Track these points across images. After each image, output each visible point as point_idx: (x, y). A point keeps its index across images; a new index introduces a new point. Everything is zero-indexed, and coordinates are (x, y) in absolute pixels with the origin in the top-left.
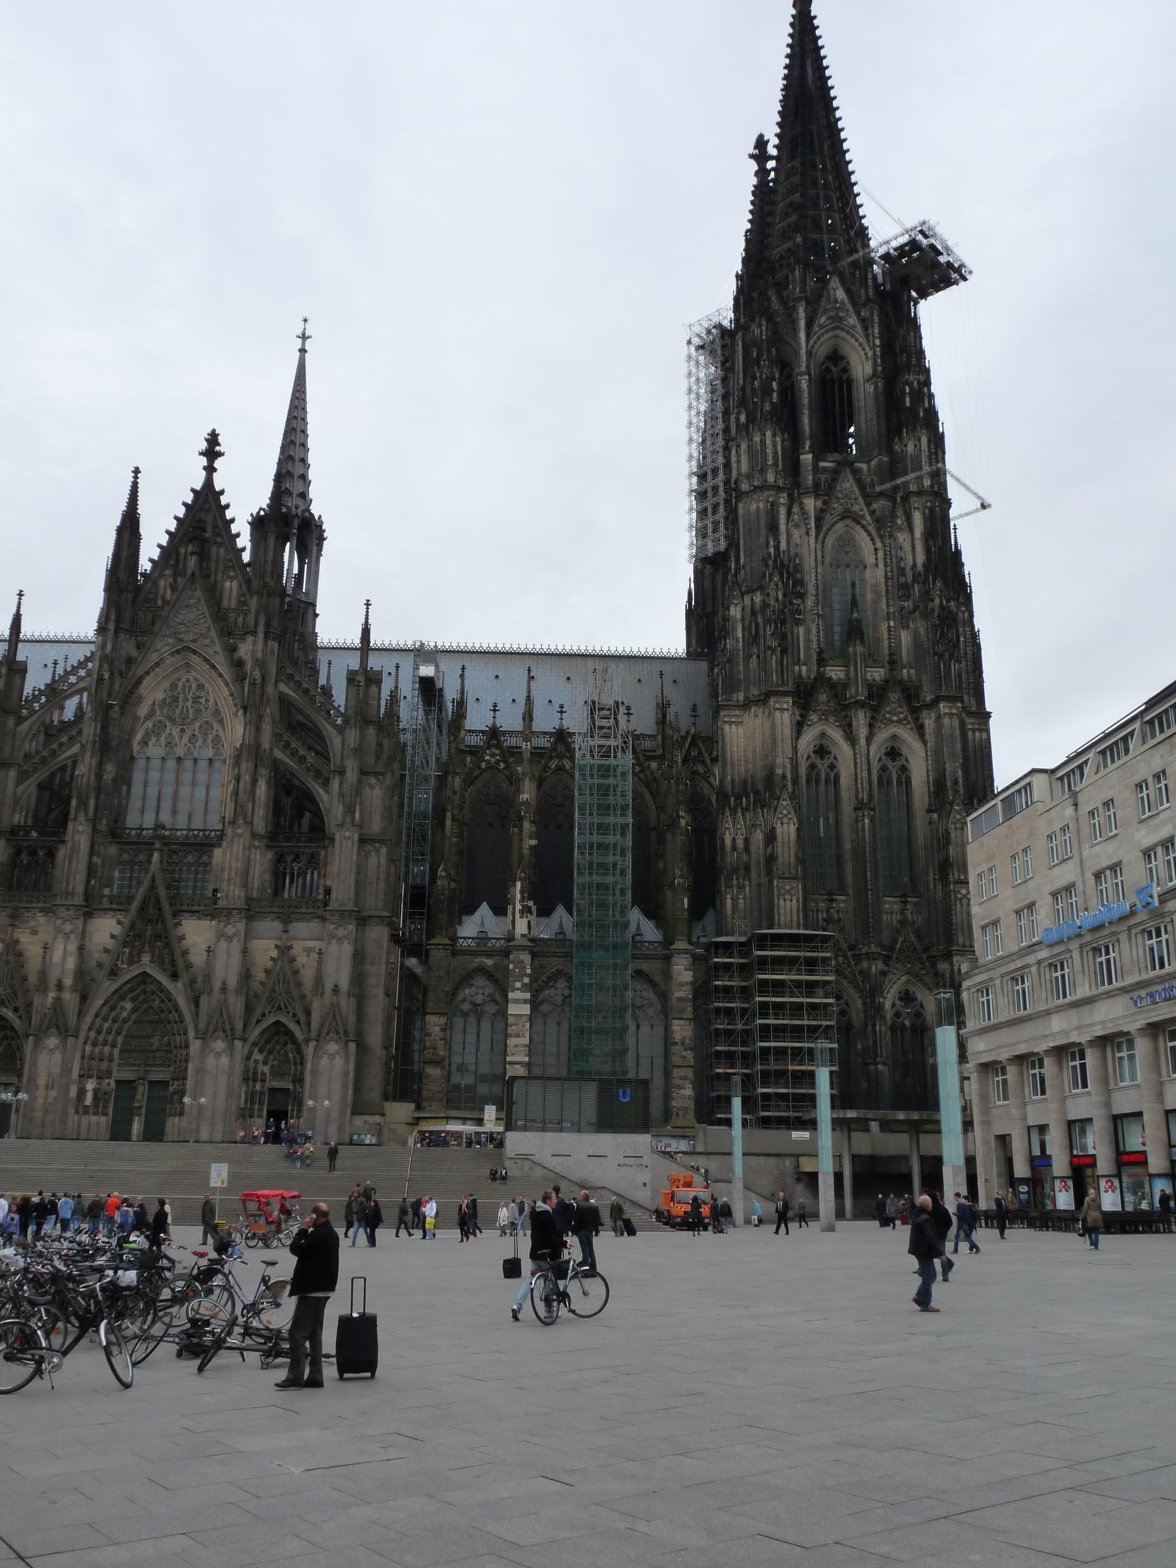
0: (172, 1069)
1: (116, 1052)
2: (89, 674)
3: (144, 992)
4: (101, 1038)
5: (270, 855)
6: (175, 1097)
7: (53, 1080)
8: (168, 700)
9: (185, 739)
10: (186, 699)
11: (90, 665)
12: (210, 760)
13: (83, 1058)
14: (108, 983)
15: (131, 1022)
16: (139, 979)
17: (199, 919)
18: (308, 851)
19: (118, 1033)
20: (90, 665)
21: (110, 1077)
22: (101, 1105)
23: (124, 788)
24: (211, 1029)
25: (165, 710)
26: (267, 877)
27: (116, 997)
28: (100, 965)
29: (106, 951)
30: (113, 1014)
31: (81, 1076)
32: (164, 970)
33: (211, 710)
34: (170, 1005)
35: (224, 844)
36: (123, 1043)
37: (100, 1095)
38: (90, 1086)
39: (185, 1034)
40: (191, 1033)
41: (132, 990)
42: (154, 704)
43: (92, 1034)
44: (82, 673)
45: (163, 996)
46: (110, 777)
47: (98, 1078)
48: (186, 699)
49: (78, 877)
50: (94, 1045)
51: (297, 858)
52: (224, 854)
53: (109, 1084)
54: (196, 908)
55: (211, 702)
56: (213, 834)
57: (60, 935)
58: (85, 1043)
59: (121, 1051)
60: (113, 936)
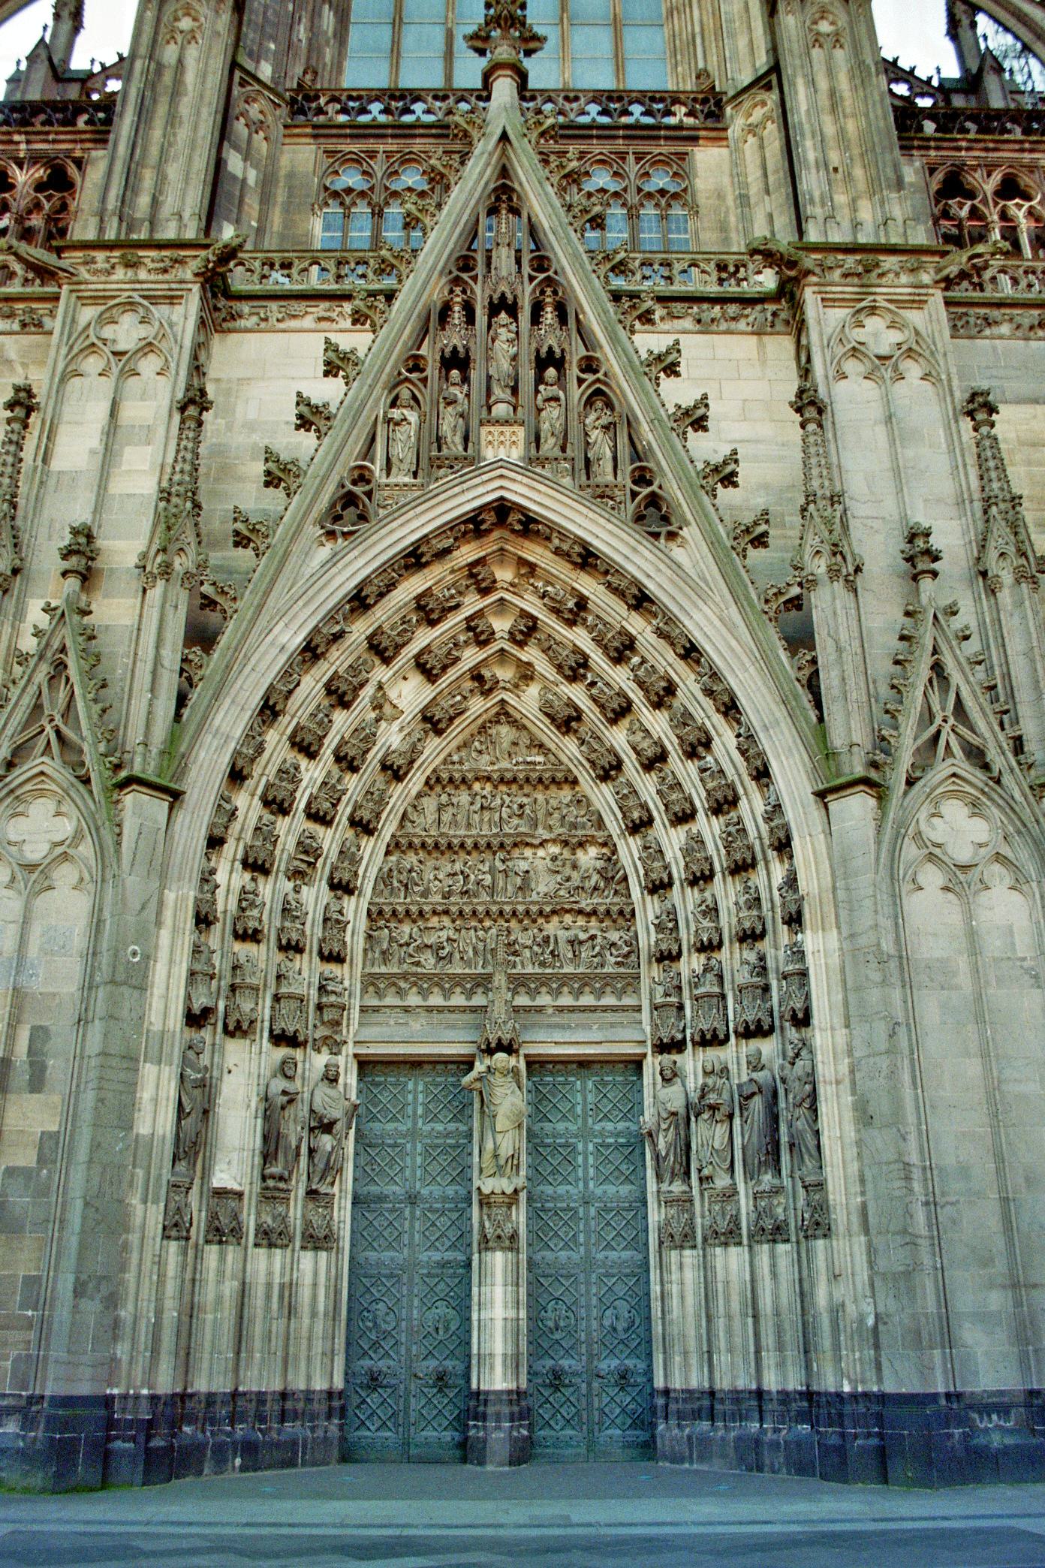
4: (290, 830)
6: (708, 1135)
7: (39, 1034)
13: (203, 920)
14: (325, 552)
15: (415, 782)
19: (363, 827)
21: (335, 1046)
22: (299, 1188)
23: (328, 19)
24: (907, 744)
27: (360, 629)
28: (279, 475)
29: (310, 417)
30: (342, 722)
31: (196, 1019)
32: (603, 495)
36: (385, 879)
37: (293, 1131)
38: (243, 1071)
41: (427, 611)
43: (247, 804)
47: (280, 1039)
49: (173, 171)
50: (256, 866)
53: (331, 1078)
57: (92, 364)
58: (215, 842)
60: (336, 364)
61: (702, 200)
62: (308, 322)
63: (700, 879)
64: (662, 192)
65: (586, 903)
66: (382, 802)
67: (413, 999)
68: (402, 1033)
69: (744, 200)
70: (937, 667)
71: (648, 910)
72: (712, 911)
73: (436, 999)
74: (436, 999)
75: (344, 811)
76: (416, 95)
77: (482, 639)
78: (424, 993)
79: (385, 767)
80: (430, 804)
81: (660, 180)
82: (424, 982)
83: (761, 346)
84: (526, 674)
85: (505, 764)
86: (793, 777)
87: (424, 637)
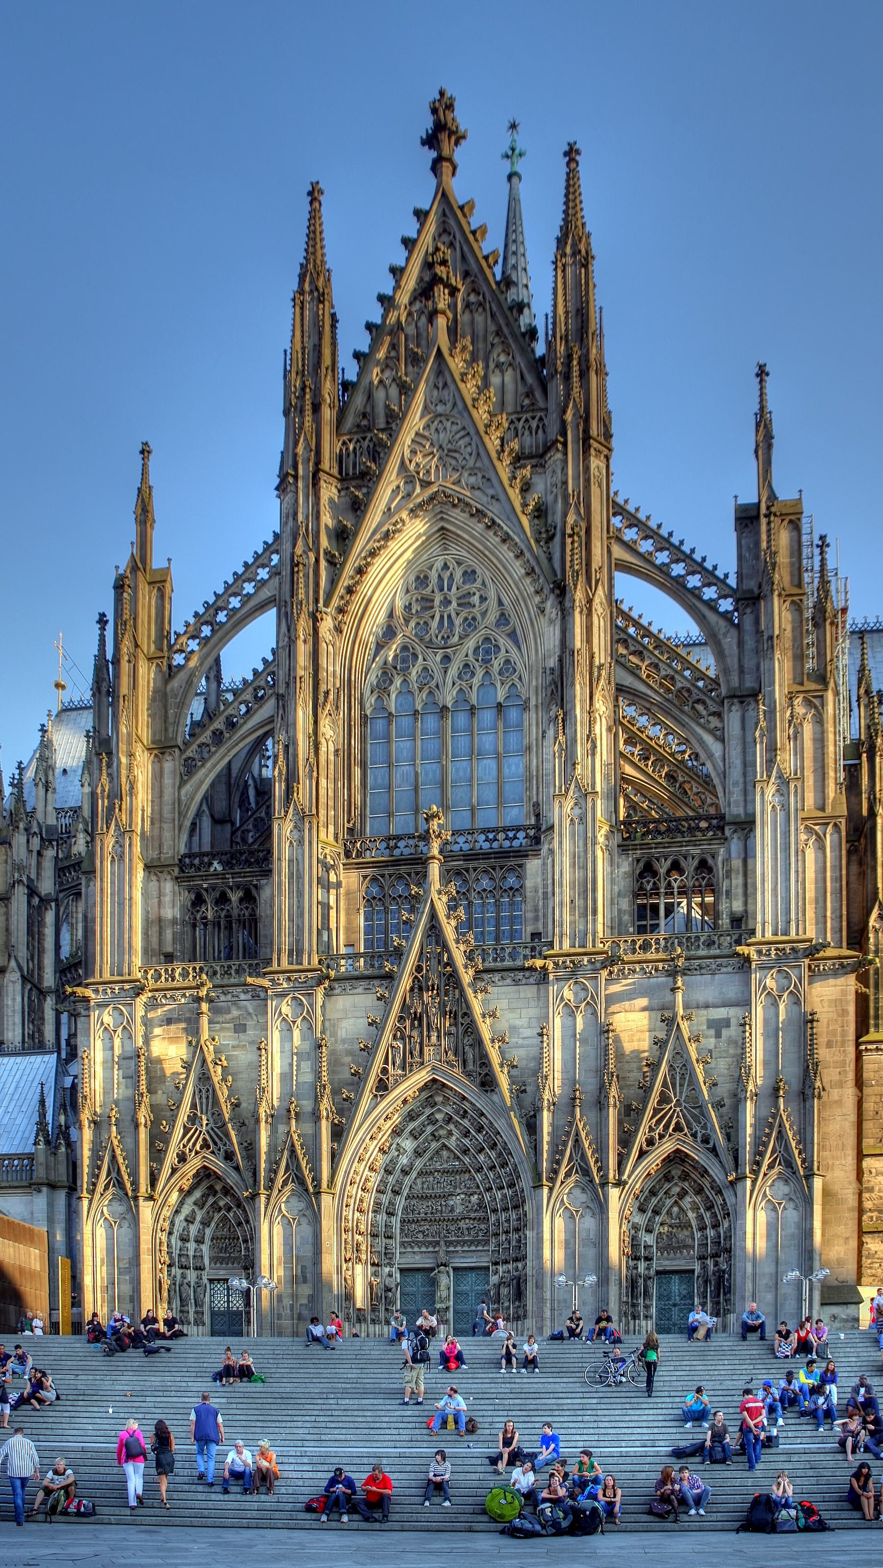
0: (492, 1247)
1: (396, 1222)
2: (275, 572)
3: (431, 1120)
5: (625, 866)
8: (415, 608)
9: (453, 671)
10: (447, 602)
11: (275, 558)
12: (499, 705)
15: (414, 1174)
16: (425, 1095)
17: (516, 983)
18: (695, 851)
19: (396, 1193)
20: (275, 558)
25: (412, 624)
26: (625, 904)
33: (493, 616)
34: (480, 1137)
35: (545, 848)
36: (405, 1209)
39: (511, 1185)
40: (526, 1182)
42: (391, 615)
44: (263, 574)
45: (466, 1123)
46: (332, 749)
48: (447, 602)
51: (676, 866)
52: (544, 864)
54: (508, 963)
55: (493, 603)
56: (521, 835)
59: (403, 1222)
61: (528, 894)
62: (360, 990)
63: (506, 1209)
64: (511, 888)
65: (473, 1215)
66: (402, 1184)
67: (416, 1249)
68: (412, 1261)
69: (545, 894)
70: (577, 1141)
71: (493, 1218)
72: (508, 1221)
73: (423, 1249)
74: (423, 1249)
75: (389, 1188)
76: (399, 838)
77: (434, 1122)
78: (420, 1247)
79: (402, 1171)
80: (419, 1181)
81: (511, 881)
82: (419, 1244)
83: (539, 990)
84: (450, 1133)
85: (445, 1166)
86: (526, 1182)
87: (411, 1126)
